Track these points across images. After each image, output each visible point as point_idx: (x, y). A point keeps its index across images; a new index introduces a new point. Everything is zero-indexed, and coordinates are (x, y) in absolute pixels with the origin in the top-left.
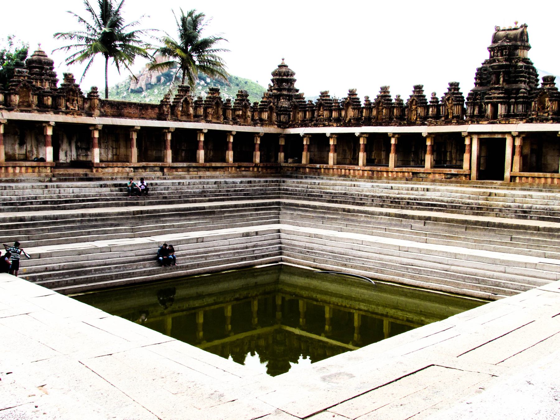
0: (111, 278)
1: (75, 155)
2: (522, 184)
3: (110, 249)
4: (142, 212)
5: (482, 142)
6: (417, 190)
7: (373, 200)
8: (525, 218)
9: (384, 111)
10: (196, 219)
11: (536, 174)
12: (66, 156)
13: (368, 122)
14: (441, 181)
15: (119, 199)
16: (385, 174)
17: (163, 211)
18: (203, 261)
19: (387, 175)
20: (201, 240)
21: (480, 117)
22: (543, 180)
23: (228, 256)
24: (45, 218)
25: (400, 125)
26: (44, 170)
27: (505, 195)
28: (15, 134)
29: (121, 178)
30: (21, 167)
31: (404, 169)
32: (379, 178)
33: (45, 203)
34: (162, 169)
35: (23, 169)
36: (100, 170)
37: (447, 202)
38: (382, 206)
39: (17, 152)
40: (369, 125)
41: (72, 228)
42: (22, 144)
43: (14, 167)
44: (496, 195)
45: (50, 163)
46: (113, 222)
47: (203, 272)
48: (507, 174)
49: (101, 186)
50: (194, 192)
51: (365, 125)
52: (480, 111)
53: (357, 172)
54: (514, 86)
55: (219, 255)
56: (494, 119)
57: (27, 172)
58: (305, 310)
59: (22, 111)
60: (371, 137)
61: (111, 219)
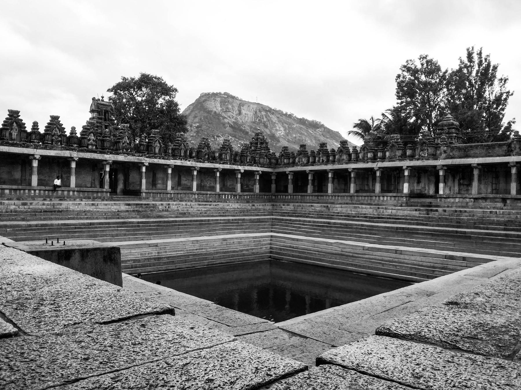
0: (310, 259)
1: (457, 190)
3: (331, 244)
4: (403, 228)
10: (443, 240)
12: (450, 190)
15: (422, 220)
17: (422, 230)
18: (380, 266)
20: (400, 252)
23: (404, 268)
24: (341, 224)
26: (402, 199)
28: (415, 176)
29: (456, 206)
30: (387, 196)
33: (366, 217)
34: (504, 200)
35: (389, 198)
36: (443, 200)
39: (416, 188)
41: (346, 232)
42: (419, 182)
43: (383, 196)
45: (405, 194)
46: (377, 232)
47: (366, 272)
49: (416, 210)
50: (497, 220)
55: (396, 266)
57: (391, 200)
58: (310, 302)
59: (389, 161)
61: (375, 230)
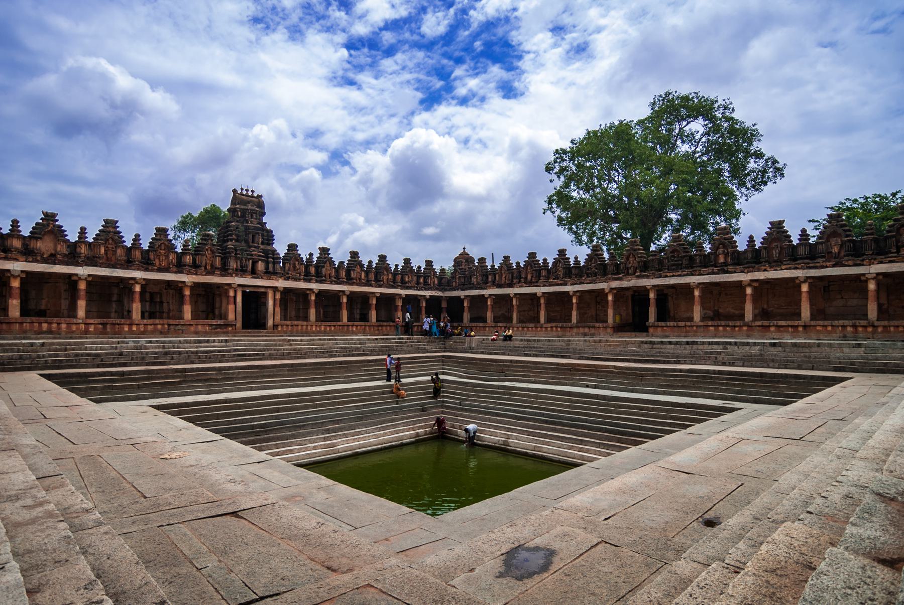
2: (286, 332)
5: (244, 293)
6: (214, 341)
7: (172, 358)
8: (335, 356)
9: (119, 251)
11: (296, 323)
13: (92, 261)
14: (205, 333)
16: (126, 329)
19: (130, 329)
21: (242, 271)
22: (300, 327)
25: (146, 270)
27: (301, 340)
31: (157, 321)
32: (118, 334)
37: (260, 350)
38: (193, 363)
40: (96, 266)
44: (293, 340)
48: (270, 323)
51: (87, 265)
52: (241, 266)
53: (74, 328)
54: (269, 248)
56: (254, 273)
60: (94, 282)
